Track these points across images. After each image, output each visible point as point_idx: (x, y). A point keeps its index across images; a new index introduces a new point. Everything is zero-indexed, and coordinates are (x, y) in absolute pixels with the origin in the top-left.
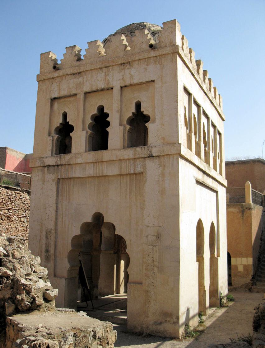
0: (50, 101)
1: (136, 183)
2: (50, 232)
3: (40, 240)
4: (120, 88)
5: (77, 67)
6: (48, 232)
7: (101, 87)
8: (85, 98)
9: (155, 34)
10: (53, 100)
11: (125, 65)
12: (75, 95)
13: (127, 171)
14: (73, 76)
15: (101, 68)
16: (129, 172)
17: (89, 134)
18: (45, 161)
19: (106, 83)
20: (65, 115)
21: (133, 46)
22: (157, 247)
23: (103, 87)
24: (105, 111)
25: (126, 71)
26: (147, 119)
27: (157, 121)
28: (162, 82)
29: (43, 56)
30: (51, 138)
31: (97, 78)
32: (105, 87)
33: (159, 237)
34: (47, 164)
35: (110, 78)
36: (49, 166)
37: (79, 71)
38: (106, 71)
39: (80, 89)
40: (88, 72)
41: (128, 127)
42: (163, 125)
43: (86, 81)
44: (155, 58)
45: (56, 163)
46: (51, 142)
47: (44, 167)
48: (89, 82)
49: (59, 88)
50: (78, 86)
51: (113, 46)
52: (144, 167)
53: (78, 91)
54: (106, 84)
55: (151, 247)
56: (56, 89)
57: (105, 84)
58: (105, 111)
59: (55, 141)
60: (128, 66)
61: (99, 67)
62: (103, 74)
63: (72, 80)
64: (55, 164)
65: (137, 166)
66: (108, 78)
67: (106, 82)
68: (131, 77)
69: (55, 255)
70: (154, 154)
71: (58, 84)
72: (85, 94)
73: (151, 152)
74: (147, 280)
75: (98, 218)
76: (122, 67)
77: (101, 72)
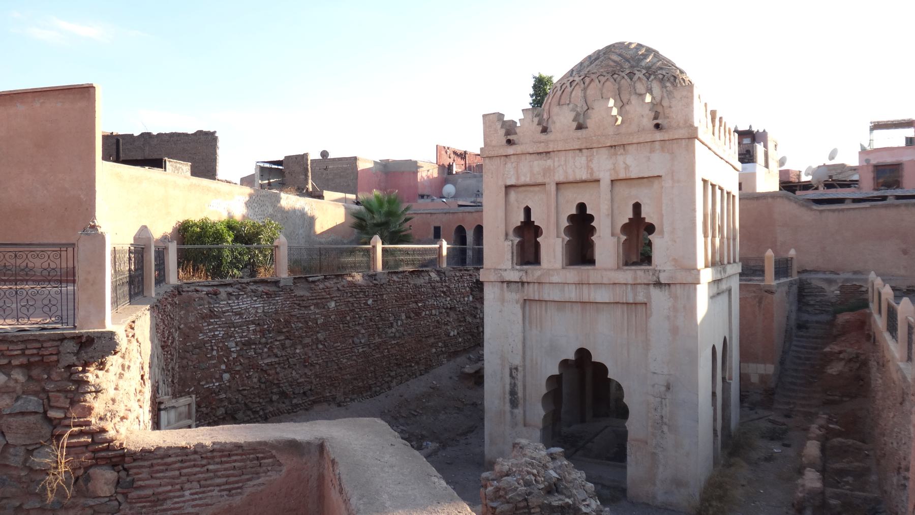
0: (504, 189)
1: (636, 316)
2: (516, 369)
3: (502, 378)
4: (610, 182)
5: (542, 144)
6: (513, 370)
8: (557, 189)
9: (650, 75)
10: (508, 188)
11: (616, 148)
12: (544, 184)
13: (624, 299)
14: (537, 157)
15: (580, 150)
16: (626, 299)
17: (565, 242)
18: (503, 275)
19: (589, 172)
20: (528, 211)
21: (629, 120)
22: (667, 400)
23: (584, 177)
24: (588, 212)
25: (619, 157)
26: (651, 229)
27: (666, 235)
29: (486, 119)
30: (510, 243)
31: (574, 163)
33: (669, 389)
34: (507, 279)
35: (594, 165)
36: (509, 282)
37: (546, 150)
39: (549, 177)
41: (624, 238)
42: (675, 242)
43: (559, 166)
44: (662, 142)
45: (520, 279)
46: (510, 248)
47: (503, 282)
48: (563, 168)
49: (517, 172)
50: (547, 171)
52: (649, 296)
53: (547, 180)
54: (589, 174)
55: (659, 399)
56: (512, 173)
57: (587, 173)
58: (588, 212)
59: (515, 247)
60: (622, 151)
61: (577, 147)
62: (584, 158)
63: (536, 163)
64: (519, 281)
65: (638, 294)
66: (592, 166)
67: (589, 171)
68: (627, 167)
69: (525, 400)
70: (663, 281)
71: (514, 164)
72: (557, 184)
73: (659, 278)
74: (654, 440)
75: (583, 354)
76: (613, 150)
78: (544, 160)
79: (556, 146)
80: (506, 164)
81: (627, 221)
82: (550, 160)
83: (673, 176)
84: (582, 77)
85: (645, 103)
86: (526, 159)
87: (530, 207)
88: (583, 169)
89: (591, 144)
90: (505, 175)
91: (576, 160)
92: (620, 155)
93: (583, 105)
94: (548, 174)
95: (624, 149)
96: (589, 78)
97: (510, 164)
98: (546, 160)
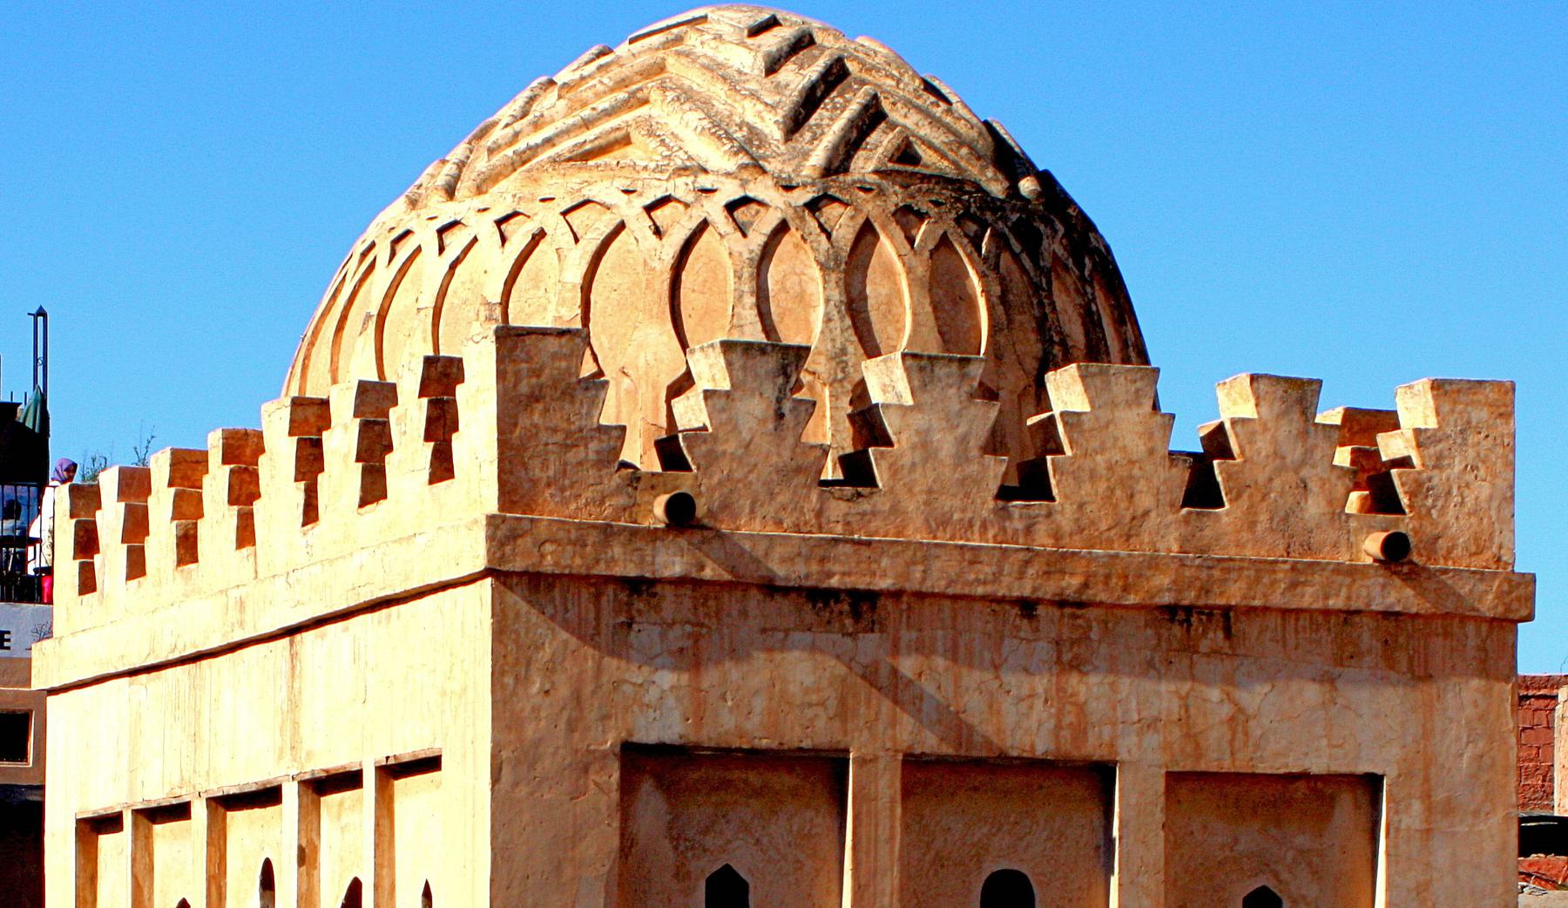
4: (1161, 785)
7: (1033, 747)
28: (1427, 796)
32: (1058, 748)
38: (1066, 634)
40: (928, 608)
44: (1390, 625)
51: (1095, 444)
67: (1069, 719)
68: (1238, 720)
80: (630, 625)
82: (875, 636)
83: (1427, 780)
84: (802, 196)
85: (1317, 425)
86: (744, 613)
88: (1039, 704)
89: (1086, 585)
90: (627, 688)
91: (1005, 651)
92: (1207, 655)
93: (843, 351)
95: (1228, 634)
96: (849, 211)
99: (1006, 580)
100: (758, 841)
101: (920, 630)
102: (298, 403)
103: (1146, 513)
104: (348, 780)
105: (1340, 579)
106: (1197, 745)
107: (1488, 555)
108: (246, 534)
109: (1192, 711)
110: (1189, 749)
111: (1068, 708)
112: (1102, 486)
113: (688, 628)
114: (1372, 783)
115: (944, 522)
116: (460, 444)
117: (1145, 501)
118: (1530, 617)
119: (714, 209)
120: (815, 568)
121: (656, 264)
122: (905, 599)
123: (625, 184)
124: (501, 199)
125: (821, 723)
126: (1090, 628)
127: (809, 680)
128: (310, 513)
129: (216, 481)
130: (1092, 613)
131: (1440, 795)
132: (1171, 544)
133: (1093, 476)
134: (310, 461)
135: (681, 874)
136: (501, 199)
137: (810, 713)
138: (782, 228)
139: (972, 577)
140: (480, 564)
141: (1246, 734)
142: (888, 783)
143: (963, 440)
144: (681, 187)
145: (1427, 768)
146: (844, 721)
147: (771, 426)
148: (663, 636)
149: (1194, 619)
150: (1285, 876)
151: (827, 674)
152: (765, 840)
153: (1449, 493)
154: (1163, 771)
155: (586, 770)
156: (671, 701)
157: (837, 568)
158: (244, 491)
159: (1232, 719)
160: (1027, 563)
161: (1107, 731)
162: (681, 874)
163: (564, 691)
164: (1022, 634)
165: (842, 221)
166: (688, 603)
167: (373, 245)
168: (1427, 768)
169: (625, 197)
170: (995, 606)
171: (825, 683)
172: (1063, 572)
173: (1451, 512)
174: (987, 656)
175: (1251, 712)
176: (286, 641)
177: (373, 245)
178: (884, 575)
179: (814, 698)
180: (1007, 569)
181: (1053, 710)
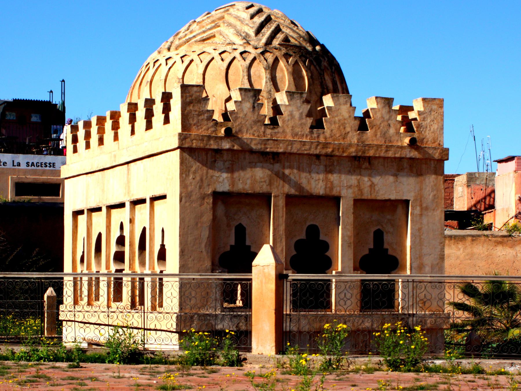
4: (352, 203)
7: (319, 193)
28: (421, 205)
32: (326, 193)
38: (328, 163)
51: (335, 114)
60: (366, 164)
67: (329, 185)
77: (317, 162)
78: (271, 164)
79: (289, 148)
80: (215, 161)
81: (367, 252)
83: (421, 201)
84: (260, 51)
85: (392, 110)
86: (245, 158)
87: (244, 225)
88: (321, 182)
89: (333, 151)
90: (215, 178)
92: (364, 169)
93: (270, 91)
94: (275, 183)
95: (370, 163)
96: (272, 54)
97: (222, 163)
98: (273, 164)
99: (312, 150)
100: (248, 217)
101: (290, 163)
102: (130, 104)
103: (348, 132)
104: (142, 201)
105: (398, 149)
106: (362, 192)
107: (436, 143)
108: (116, 138)
109: (360, 183)
110: (360, 193)
111: (328, 183)
112: (337, 125)
113: (230, 162)
114: (407, 202)
115: (296, 135)
116: (171, 114)
117: (348, 129)
118: (447, 159)
119: (237, 54)
120: (263, 146)
121: (222, 68)
122: (286, 154)
123: (214, 47)
124: (182, 51)
125: (264, 187)
126: (334, 162)
127: (261, 176)
128: (133, 132)
129: (108, 124)
130: (335, 158)
131: (424, 205)
132: (355, 140)
133: (335, 123)
134: (133, 119)
135: (229, 225)
136: (182, 51)
137: (262, 184)
138: (254, 59)
139: (303, 149)
140: (176, 145)
141: (374, 189)
142: (282, 202)
143: (301, 114)
144: (228, 48)
145: (421, 198)
146: (271, 186)
147: (252, 110)
148: (224, 164)
149: (361, 160)
150: (384, 226)
151: (266, 174)
152: (250, 217)
153: (427, 127)
154: (353, 199)
155: (204, 199)
156: (226, 181)
157: (269, 146)
158: (116, 127)
159: (371, 186)
160: (318, 145)
161: (338, 189)
162: (229, 225)
163: (198, 178)
164: (316, 164)
165: (270, 57)
166: (230, 156)
167: (149, 64)
168: (421, 198)
169: (214, 51)
170: (309, 156)
171: (266, 176)
172: (327, 148)
173: (427, 132)
174: (307, 169)
175: (376, 183)
176: (126, 166)
177: (149, 64)
178: (281, 148)
179: (263, 180)
180: (313, 147)
181: (324, 183)
